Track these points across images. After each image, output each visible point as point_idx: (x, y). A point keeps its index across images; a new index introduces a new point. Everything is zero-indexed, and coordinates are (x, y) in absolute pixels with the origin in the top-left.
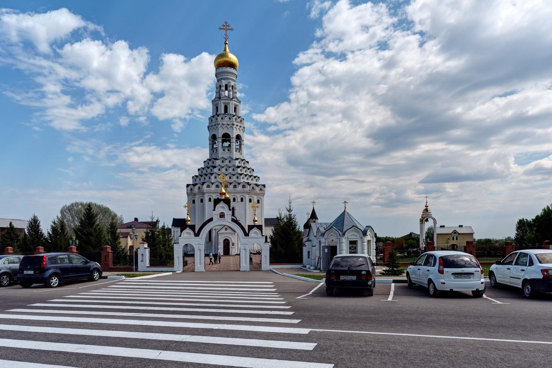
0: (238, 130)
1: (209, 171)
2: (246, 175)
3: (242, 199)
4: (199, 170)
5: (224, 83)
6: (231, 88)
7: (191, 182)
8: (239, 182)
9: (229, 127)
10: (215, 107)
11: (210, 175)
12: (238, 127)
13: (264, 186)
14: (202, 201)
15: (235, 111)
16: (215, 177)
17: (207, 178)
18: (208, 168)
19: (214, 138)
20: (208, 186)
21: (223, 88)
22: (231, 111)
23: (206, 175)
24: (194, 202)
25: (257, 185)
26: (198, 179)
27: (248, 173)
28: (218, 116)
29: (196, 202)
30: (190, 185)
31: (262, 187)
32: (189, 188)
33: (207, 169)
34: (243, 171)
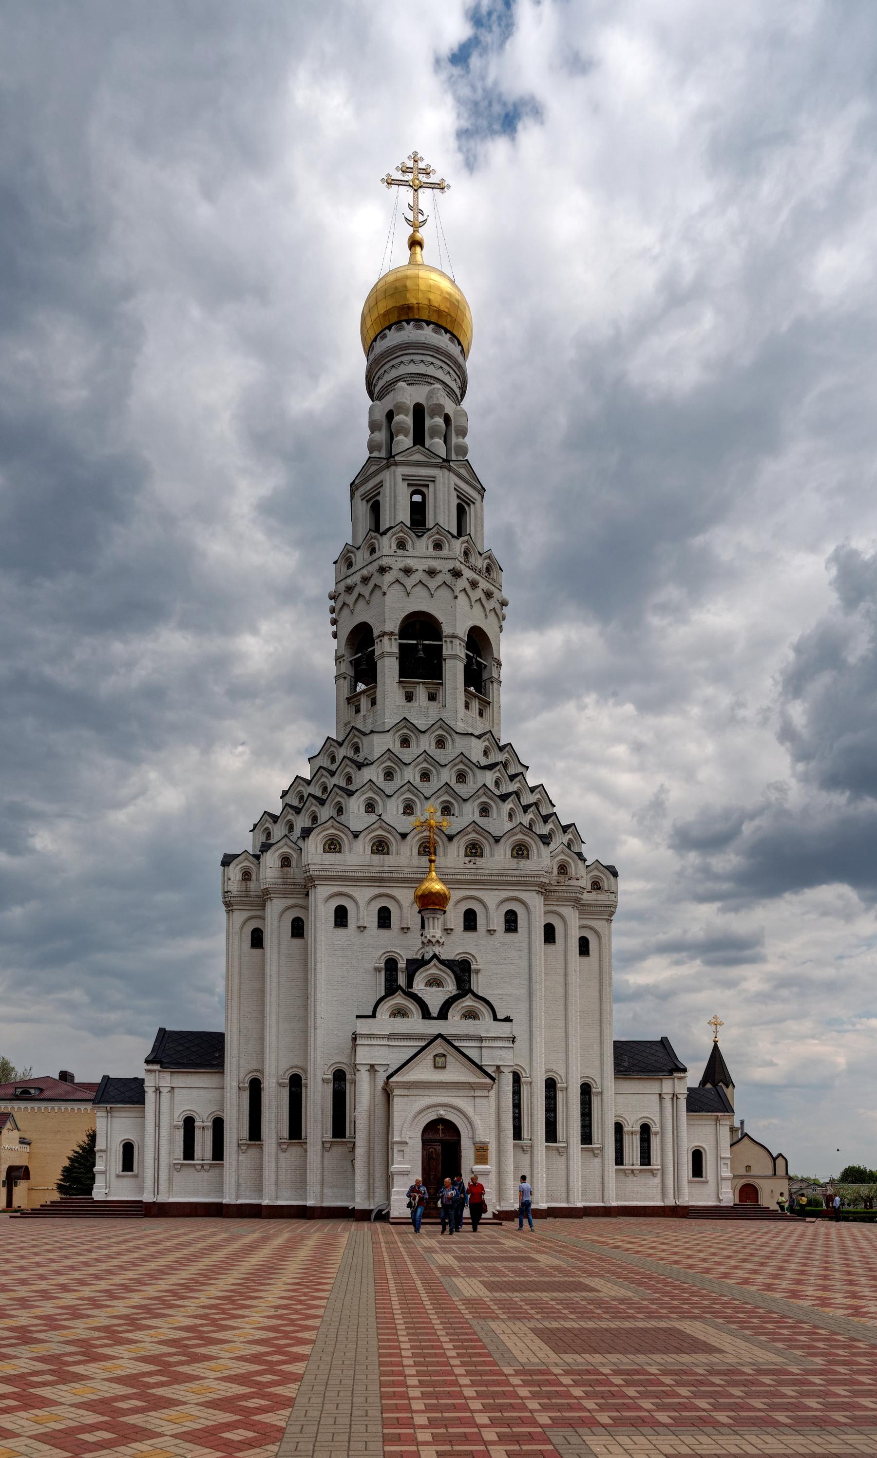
14: (298, 929)
16: (370, 807)
22: (441, 512)
24: (257, 939)
29: (269, 939)
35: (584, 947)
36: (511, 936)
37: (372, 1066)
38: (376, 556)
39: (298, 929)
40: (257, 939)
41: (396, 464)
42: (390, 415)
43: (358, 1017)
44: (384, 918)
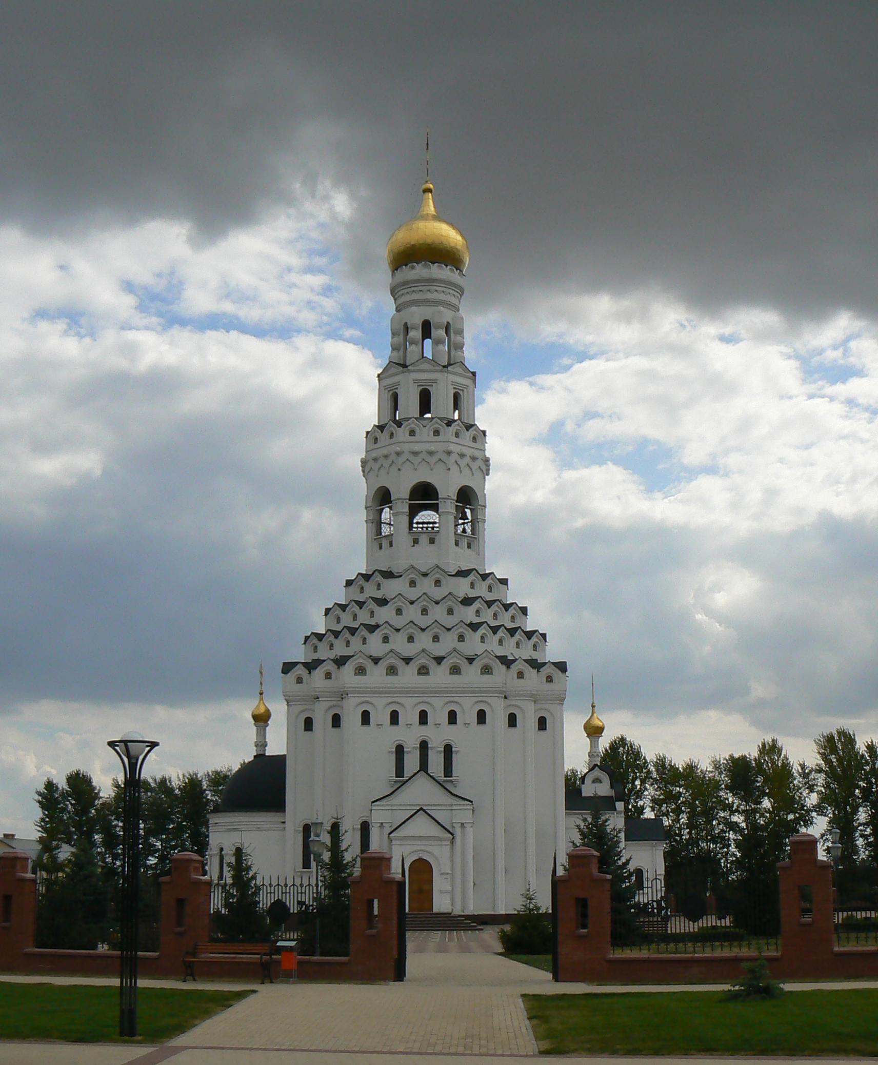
0: (466, 471)
1: (364, 617)
2: (495, 630)
3: (481, 717)
4: (327, 611)
5: (417, 315)
6: (442, 332)
7: (299, 654)
8: (470, 653)
9: (432, 460)
10: (388, 396)
11: (364, 632)
12: (467, 460)
13: (562, 667)
14: (336, 721)
15: (456, 407)
16: (386, 639)
17: (355, 641)
18: (361, 604)
19: (383, 497)
20: (361, 671)
21: (416, 334)
22: (441, 404)
23: (353, 631)
24: (309, 724)
25: (535, 665)
26: (323, 646)
27: (505, 619)
28: (399, 424)
29: (316, 725)
30: (295, 664)
31: (556, 674)
32: (292, 676)
33: (356, 608)
34: (487, 616)
35: (542, 724)
36: (481, 727)
37: (382, 823)
38: (394, 440)
39: (336, 721)
40: (309, 724)
41: (409, 371)
42: (406, 328)
43: (373, 802)
44: (394, 718)
